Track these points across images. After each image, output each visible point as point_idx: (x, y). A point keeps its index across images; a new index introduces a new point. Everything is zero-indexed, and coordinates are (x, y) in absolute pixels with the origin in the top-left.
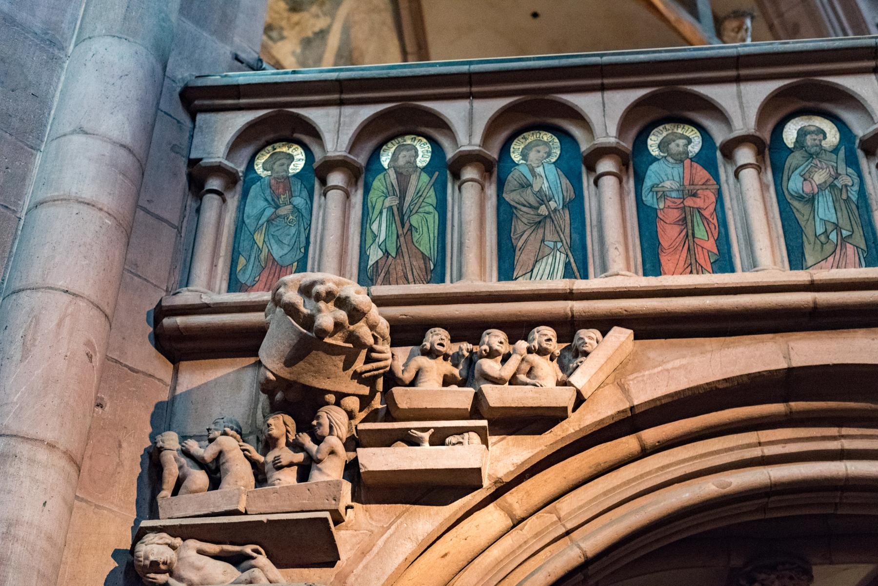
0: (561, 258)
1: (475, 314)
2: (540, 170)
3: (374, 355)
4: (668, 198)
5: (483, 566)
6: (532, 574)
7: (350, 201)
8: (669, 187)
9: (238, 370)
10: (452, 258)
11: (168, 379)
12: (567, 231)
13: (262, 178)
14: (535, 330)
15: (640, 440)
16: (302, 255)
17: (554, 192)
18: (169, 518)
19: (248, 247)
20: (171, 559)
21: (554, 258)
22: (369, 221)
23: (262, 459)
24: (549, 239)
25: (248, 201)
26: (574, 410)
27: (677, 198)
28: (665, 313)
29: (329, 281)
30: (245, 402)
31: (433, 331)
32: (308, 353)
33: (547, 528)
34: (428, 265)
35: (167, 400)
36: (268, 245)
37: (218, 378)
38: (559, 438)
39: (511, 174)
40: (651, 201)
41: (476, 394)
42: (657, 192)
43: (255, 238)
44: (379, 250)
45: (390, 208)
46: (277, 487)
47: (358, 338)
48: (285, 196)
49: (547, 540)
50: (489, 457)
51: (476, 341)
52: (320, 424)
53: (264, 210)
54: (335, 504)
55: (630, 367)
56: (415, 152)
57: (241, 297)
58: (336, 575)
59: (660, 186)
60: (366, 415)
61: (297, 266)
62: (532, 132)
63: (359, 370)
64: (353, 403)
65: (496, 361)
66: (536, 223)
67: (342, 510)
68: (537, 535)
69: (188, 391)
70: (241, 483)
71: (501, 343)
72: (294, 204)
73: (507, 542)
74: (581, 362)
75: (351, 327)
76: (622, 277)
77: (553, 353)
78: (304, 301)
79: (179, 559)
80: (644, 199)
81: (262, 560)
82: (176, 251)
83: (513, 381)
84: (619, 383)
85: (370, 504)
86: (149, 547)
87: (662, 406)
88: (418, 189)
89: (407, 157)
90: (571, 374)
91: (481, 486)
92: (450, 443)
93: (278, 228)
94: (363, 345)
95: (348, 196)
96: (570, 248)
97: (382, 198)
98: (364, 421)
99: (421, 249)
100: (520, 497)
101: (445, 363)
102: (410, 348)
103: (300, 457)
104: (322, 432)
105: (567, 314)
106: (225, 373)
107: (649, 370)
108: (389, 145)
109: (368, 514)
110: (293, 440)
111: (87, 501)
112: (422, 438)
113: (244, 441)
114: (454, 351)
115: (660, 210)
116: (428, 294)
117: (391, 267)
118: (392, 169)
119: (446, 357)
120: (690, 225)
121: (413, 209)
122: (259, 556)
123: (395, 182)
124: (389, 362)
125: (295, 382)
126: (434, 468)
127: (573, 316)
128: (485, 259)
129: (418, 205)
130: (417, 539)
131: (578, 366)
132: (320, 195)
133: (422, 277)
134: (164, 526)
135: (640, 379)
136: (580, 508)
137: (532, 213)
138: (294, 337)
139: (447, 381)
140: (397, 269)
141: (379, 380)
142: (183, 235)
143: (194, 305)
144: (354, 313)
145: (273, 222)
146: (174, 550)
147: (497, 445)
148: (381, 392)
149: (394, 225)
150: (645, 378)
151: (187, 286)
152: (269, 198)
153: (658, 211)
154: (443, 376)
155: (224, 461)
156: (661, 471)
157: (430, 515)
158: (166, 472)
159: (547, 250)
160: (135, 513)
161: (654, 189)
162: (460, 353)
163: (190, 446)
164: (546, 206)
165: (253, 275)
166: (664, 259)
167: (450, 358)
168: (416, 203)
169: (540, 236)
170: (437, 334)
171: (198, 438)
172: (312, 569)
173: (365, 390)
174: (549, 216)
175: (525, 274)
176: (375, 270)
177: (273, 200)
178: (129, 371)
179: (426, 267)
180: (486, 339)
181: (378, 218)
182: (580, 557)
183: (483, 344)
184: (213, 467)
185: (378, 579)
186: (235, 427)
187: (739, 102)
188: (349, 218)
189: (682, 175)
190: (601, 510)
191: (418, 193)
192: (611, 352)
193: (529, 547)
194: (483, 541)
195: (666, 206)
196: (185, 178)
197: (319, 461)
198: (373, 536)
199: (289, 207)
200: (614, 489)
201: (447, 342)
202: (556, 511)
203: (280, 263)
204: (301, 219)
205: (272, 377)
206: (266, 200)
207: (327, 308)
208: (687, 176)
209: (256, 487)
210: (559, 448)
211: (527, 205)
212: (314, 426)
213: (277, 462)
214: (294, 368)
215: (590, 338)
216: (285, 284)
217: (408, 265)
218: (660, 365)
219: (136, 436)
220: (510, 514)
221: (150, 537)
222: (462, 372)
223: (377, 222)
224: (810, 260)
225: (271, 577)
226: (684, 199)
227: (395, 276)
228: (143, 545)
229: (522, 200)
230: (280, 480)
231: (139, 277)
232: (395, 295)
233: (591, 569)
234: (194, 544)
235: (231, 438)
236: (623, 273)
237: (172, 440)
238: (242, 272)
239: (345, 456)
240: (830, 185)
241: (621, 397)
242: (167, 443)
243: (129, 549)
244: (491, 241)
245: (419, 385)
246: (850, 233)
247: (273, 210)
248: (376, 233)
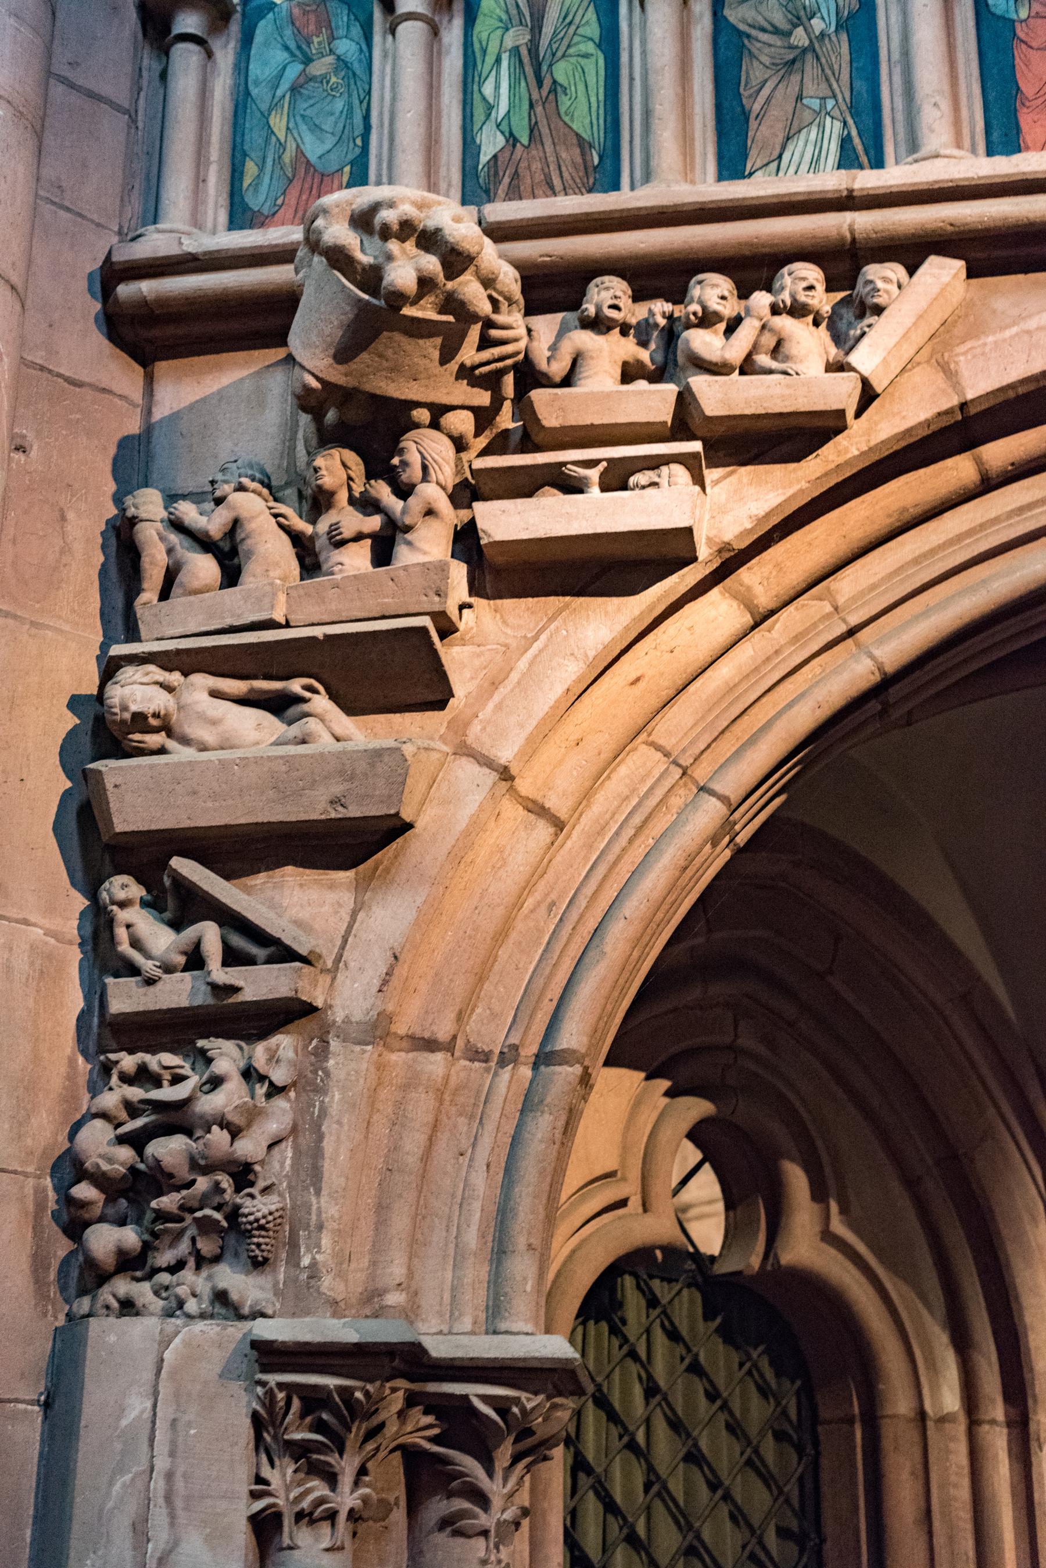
0: (833, 129)
1: (676, 245)
3: (494, 333)
5: (704, 697)
6: (790, 706)
7: (440, 40)
9: (257, 373)
10: (631, 142)
11: (137, 395)
13: (275, 4)
14: (785, 270)
15: (979, 462)
16: (358, 151)
18: (158, 639)
19: (261, 141)
20: (166, 709)
22: (477, 79)
23: (308, 529)
24: (812, 94)
25: (253, 52)
26: (858, 414)
28: (1026, 225)
29: (403, 200)
30: (273, 430)
31: (599, 283)
32: (376, 335)
33: (815, 625)
34: (588, 158)
35: (137, 431)
36: (296, 135)
37: (223, 389)
38: (832, 466)
41: (680, 395)
43: (272, 123)
44: (498, 133)
45: (515, 51)
46: (338, 577)
47: (462, 304)
49: (815, 647)
50: (708, 507)
51: (678, 296)
52: (405, 464)
53: (284, 68)
54: (440, 603)
55: (959, 330)
57: (251, 239)
58: (449, 723)
60: (487, 441)
63: (468, 363)
64: (462, 422)
65: (716, 332)
66: (787, 63)
67: (453, 612)
68: (796, 639)
69: (173, 414)
70: (275, 573)
71: (723, 298)
72: (338, 52)
73: (746, 653)
74: (869, 326)
76: (946, 160)
77: (817, 312)
78: (361, 241)
79: (180, 708)
81: (321, 703)
82: (129, 157)
83: (748, 367)
84: (940, 360)
85: (501, 597)
86: (127, 690)
87: (1019, 398)
90: (851, 349)
91: (695, 559)
92: (637, 486)
93: (311, 102)
94: (474, 318)
95: (435, 31)
96: (850, 108)
97: (499, 32)
98: (484, 453)
99: (574, 127)
100: (765, 574)
101: (623, 340)
102: (560, 316)
103: (374, 522)
104: (409, 477)
105: (843, 238)
106: (236, 379)
107: (994, 333)
109: (498, 616)
110: (361, 493)
111: (15, 617)
112: (586, 478)
113: (276, 500)
114: (641, 318)
115: (1021, 22)
116: (587, 214)
119: (625, 329)
121: (557, 49)
122: (316, 696)
124: (522, 345)
125: (356, 390)
126: (610, 531)
127: (854, 240)
128: (693, 139)
129: (565, 42)
130: (586, 656)
131: (863, 334)
132: (385, 33)
133: (578, 180)
134: (150, 654)
135: (978, 351)
136: (873, 587)
137: (779, 43)
138: (348, 308)
139: (629, 373)
140: (533, 169)
141: (506, 377)
142: (140, 125)
144: (453, 258)
145: (302, 91)
146: (170, 692)
147: (721, 485)
148: (512, 400)
149: (523, 84)
150: (987, 349)
151: (155, 222)
152: (292, 45)
153: (1017, 25)
154: (620, 364)
155: (243, 536)
156: (1019, 515)
157: (606, 613)
158: (145, 561)
159: (807, 116)
160: (101, 632)
162: (651, 321)
163: (184, 513)
164: (805, 30)
165: (272, 194)
166: (1025, 119)
167: (632, 331)
168: (562, 38)
169: (794, 89)
170: (607, 289)
171: (196, 497)
172: (407, 714)
173: (483, 398)
174: (811, 48)
175: (767, 165)
176: (492, 172)
177: (299, 47)
178: (66, 385)
180: (696, 292)
181: (494, 73)
182: (873, 673)
183: (692, 301)
184: (226, 546)
185: (522, 726)
186: (258, 475)
188: (439, 74)
190: (909, 590)
191: (564, 19)
192: (924, 304)
193: (784, 659)
194: (702, 653)
196: (135, 15)
197: (408, 529)
198: (509, 654)
199: (330, 59)
200: (933, 552)
201: (625, 302)
202: (830, 596)
203: (320, 167)
204: (352, 82)
205: (315, 384)
206: (286, 48)
209: (302, 579)
210: (832, 484)
211: (769, 28)
212: (395, 466)
213: (334, 533)
214: (353, 365)
215: (886, 280)
216: (325, 211)
217: (551, 159)
218: (1014, 323)
219: (89, 499)
220: (748, 605)
221: (128, 673)
222: (655, 355)
225: (339, 731)
227: (528, 181)
228: (117, 686)
229: (760, 19)
230: (341, 564)
231: (68, 209)
232: (528, 219)
233: (894, 692)
234: (202, 681)
235: (252, 495)
236: (948, 152)
237: (151, 502)
238: (251, 189)
239: (451, 517)
241: (943, 386)
242: (142, 508)
243: (95, 693)
244: (703, 103)
245: (578, 383)
247: (301, 67)
248: (491, 100)
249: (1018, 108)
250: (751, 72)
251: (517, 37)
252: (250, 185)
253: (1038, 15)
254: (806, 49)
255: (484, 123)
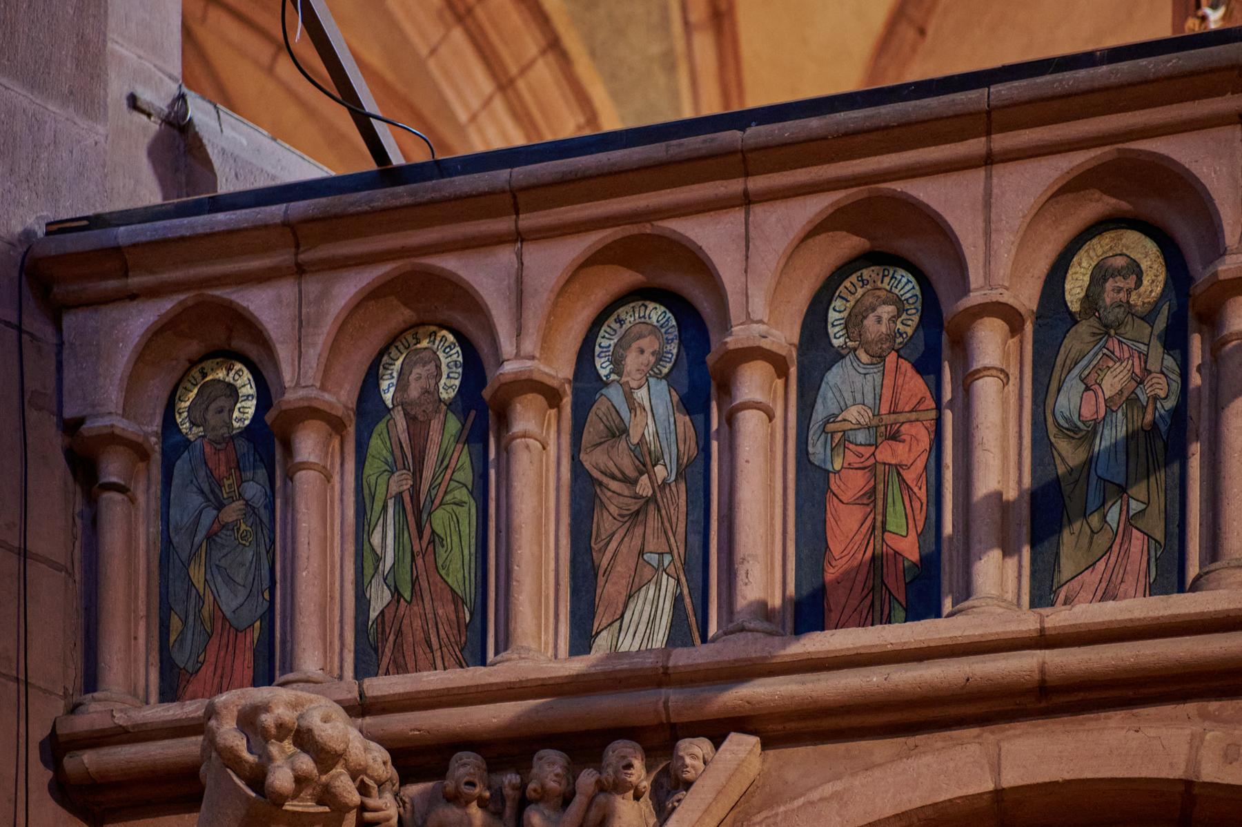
0: (668, 584)
2: (641, 395)
4: (851, 446)
8: (854, 422)
12: (681, 529)
16: (266, 605)
17: (664, 444)
21: (658, 587)
22: (366, 527)
24: (652, 549)
25: (172, 496)
27: (865, 445)
34: (461, 615)
36: (213, 588)
39: (594, 408)
40: (822, 456)
42: (833, 433)
45: (399, 497)
48: (231, 481)
53: (201, 513)
56: (436, 366)
59: (839, 419)
61: (261, 628)
62: (632, 305)
66: (632, 514)
72: (247, 496)
75: (324, 778)
80: (811, 450)
88: (443, 450)
89: (423, 380)
93: (225, 551)
94: (346, 808)
99: (450, 581)
108: (394, 352)
115: (836, 472)
117: (405, 622)
118: (400, 408)
120: (880, 503)
123: (404, 437)
129: (443, 488)
137: (626, 493)
140: (415, 625)
143: (103, 730)
145: (217, 539)
152: (206, 488)
153: (831, 475)
161: (830, 427)
164: (650, 478)
168: (440, 484)
169: (637, 542)
174: (652, 500)
175: (610, 625)
176: (380, 630)
177: (212, 491)
179: (457, 617)
187: (985, 221)
189: (878, 390)
195: (845, 465)
199: (239, 504)
206: (202, 492)
207: (282, 751)
208: (887, 394)
211: (620, 476)
217: (430, 616)
223: (379, 529)
224: (1067, 568)
226: (877, 447)
229: (611, 464)
236: (752, 626)
238: (177, 645)
240: (1127, 399)
246: (1143, 506)
247: (215, 512)
249: (826, 568)
250: (601, 525)
251: (401, 482)
252: (175, 641)
253: (850, 467)
254: (650, 498)
255: (373, 577)
